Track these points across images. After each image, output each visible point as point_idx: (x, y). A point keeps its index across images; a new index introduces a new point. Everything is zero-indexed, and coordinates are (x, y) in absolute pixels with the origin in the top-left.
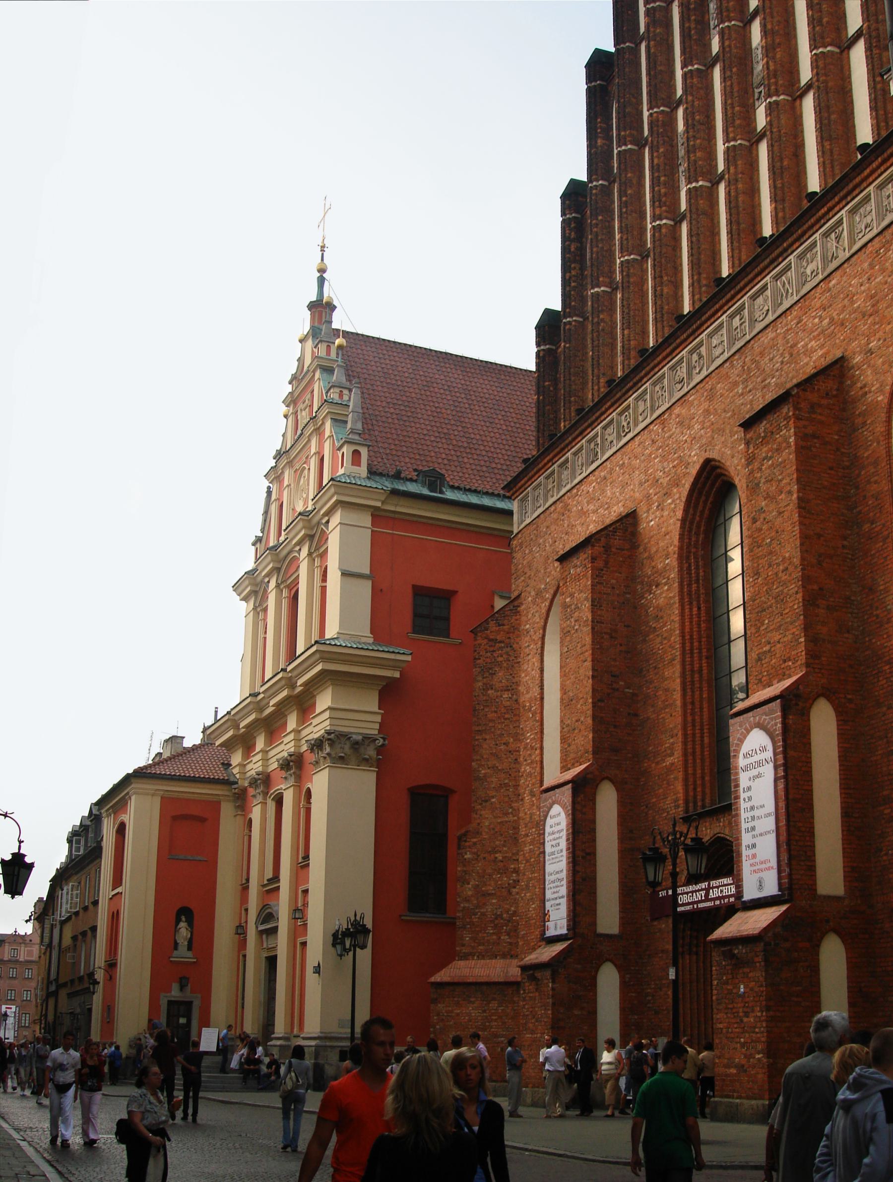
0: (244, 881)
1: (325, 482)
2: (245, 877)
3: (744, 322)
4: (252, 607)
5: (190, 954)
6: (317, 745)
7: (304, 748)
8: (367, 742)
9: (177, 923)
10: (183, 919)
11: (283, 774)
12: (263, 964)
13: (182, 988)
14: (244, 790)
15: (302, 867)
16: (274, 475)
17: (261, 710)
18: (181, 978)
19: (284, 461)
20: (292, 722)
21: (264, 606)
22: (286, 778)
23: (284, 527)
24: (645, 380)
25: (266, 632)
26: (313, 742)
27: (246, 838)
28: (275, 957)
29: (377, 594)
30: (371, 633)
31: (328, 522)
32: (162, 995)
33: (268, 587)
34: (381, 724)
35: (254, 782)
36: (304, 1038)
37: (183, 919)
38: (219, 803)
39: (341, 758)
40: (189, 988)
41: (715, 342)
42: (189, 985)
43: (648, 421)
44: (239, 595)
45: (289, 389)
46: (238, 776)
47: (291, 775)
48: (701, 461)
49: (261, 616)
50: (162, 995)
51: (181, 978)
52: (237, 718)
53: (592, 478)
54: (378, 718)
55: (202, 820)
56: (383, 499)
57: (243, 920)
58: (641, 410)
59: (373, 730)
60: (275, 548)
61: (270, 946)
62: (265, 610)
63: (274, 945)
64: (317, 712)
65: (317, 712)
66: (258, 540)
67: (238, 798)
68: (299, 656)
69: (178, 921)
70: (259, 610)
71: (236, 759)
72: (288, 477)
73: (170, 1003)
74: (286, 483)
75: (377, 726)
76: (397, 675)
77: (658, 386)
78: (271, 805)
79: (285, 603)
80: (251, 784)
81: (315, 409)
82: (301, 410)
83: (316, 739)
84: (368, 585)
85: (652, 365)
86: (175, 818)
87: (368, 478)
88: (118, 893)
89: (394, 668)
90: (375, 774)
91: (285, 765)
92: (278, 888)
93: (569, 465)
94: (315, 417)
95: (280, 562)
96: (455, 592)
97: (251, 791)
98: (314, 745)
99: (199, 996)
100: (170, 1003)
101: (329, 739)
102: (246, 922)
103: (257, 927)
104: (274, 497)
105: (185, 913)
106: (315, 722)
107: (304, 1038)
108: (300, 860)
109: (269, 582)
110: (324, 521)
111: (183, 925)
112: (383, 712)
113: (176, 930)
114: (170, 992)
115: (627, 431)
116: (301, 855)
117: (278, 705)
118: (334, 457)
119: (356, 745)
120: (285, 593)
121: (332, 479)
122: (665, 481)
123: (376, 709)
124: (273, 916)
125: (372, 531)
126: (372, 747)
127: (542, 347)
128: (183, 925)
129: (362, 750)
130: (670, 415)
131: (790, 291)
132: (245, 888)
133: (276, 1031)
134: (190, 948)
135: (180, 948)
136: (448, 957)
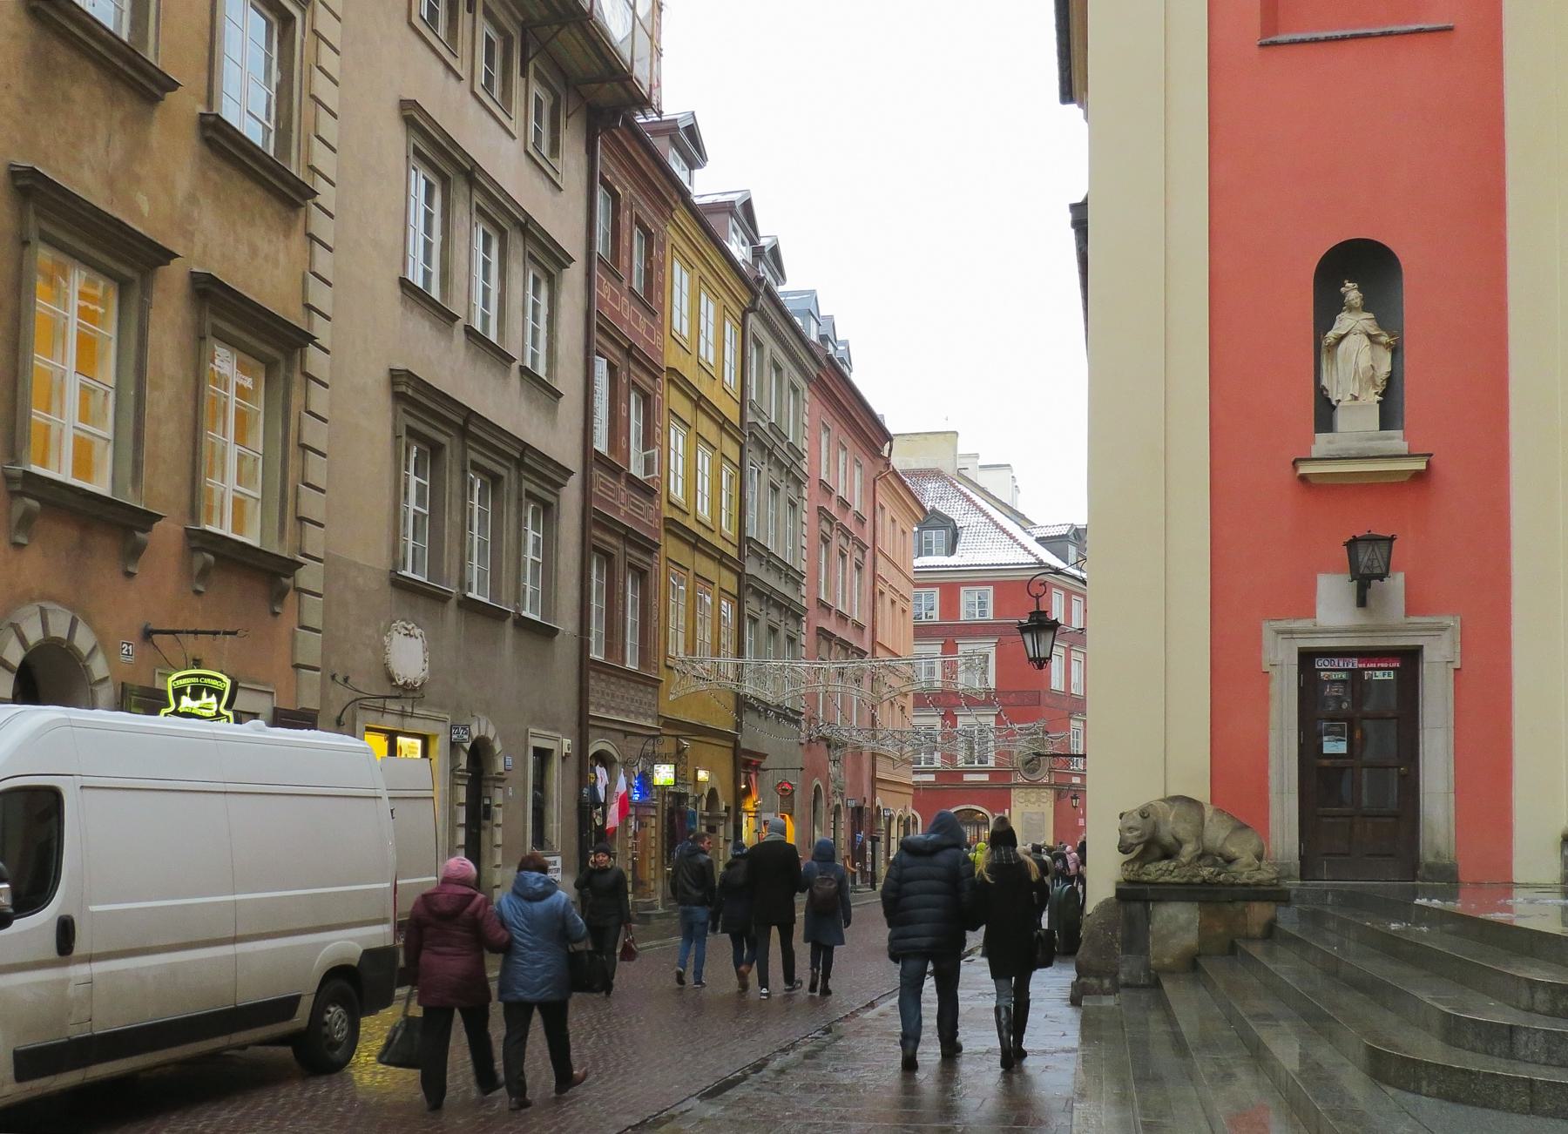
5: (1396, 441)
10: (1352, 293)
13: (1364, 585)
18: (1352, 544)
37: (1352, 293)
40: (1397, 582)
50: (1268, 628)
51: (1352, 544)
69: (1327, 307)
99: (1448, 620)
100: (1307, 658)
111: (1353, 323)
113: (1322, 349)
114: (1310, 613)
128: (1353, 323)
134: (1389, 417)
135: (1342, 419)
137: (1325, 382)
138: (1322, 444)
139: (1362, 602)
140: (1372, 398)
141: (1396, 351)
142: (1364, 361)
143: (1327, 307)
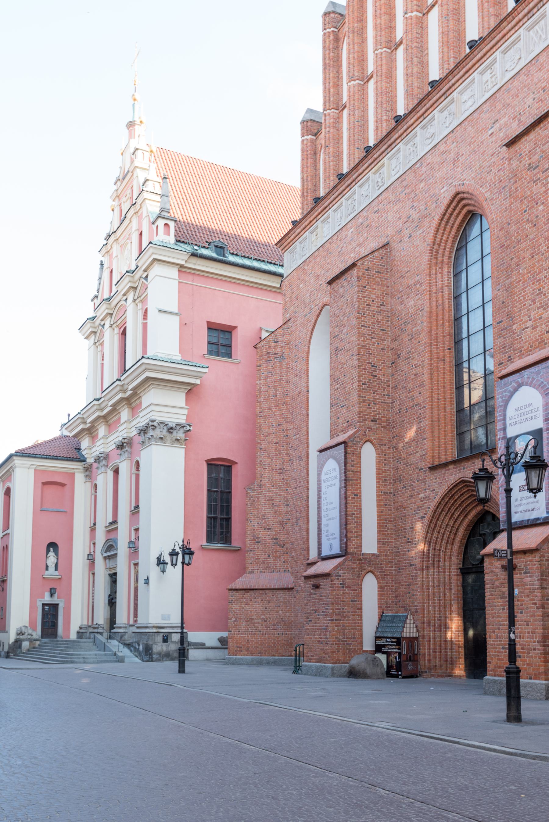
0: (92, 525)
1: (144, 244)
2: (92, 522)
3: (494, 75)
4: (93, 343)
6: (143, 431)
7: (135, 433)
8: (178, 427)
9: (47, 554)
10: (51, 549)
11: (119, 451)
12: (108, 578)
13: (52, 595)
14: (91, 465)
15: (133, 514)
16: (106, 249)
17: (102, 410)
18: (51, 589)
19: (112, 238)
20: (125, 414)
21: (101, 341)
22: (121, 454)
23: (114, 282)
24: (398, 141)
25: (103, 360)
26: (140, 428)
27: (93, 497)
28: (115, 574)
29: (183, 325)
30: (180, 353)
31: (147, 277)
32: (38, 600)
33: (103, 328)
34: (187, 416)
35: (98, 460)
36: (138, 628)
37: (51, 549)
38: (73, 474)
39: (161, 438)
41: (465, 97)
42: (56, 593)
43: (401, 173)
44: (83, 335)
45: (115, 188)
46: (86, 456)
47: (124, 452)
48: (453, 192)
49: (100, 348)
50: (38, 600)
51: (51, 589)
52: (85, 416)
53: (350, 225)
54: (186, 412)
55: (63, 485)
56: (186, 259)
57: (92, 550)
58: (393, 167)
59: (182, 420)
60: (109, 299)
61: (111, 567)
62: (102, 344)
63: (115, 566)
64: (143, 408)
65: (143, 408)
66: (96, 297)
67: (86, 471)
68: (128, 370)
69: (48, 551)
70: (99, 344)
71: (85, 444)
72: (115, 249)
73: (44, 605)
74: (114, 255)
75: (185, 417)
76: (198, 382)
77: (410, 145)
78: (110, 474)
79: (117, 338)
80: (96, 461)
81: (135, 197)
82: (124, 202)
83: (143, 426)
84: (177, 318)
85: (405, 127)
86: (44, 484)
87: (176, 244)
88: (6, 534)
89: (197, 377)
90: (183, 450)
91: (121, 446)
92: (116, 529)
93: (330, 220)
94: (135, 204)
95: (112, 309)
96: (235, 328)
97: (95, 465)
98: (142, 430)
99: (63, 600)
100: (44, 605)
101: (152, 425)
102: (94, 552)
103: (102, 555)
104: (105, 266)
105: (53, 546)
106: (141, 414)
107: (138, 628)
108: (133, 509)
109: (104, 325)
110: (144, 276)
111: (52, 554)
112: (188, 407)
114: (44, 598)
115: (381, 184)
116: (133, 505)
117: (115, 406)
118: (150, 230)
119: (170, 430)
120: (117, 330)
121: (150, 243)
122: (415, 215)
123: (183, 404)
124: (114, 547)
125: (179, 282)
126: (182, 430)
127: (306, 137)
128: (52, 554)
129: (175, 433)
130: (422, 164)
131: (543, 37)
132: (93, 529)
133: (117, 622)
134: (56, 569)
135: (49, 569)
136: (242, 571)
137: (47, 563)
138: (47, 572)
139: (51, 596)
140: (54, 566)
141: (57, 559)
142: (53, 560)
143: (48, 551)
